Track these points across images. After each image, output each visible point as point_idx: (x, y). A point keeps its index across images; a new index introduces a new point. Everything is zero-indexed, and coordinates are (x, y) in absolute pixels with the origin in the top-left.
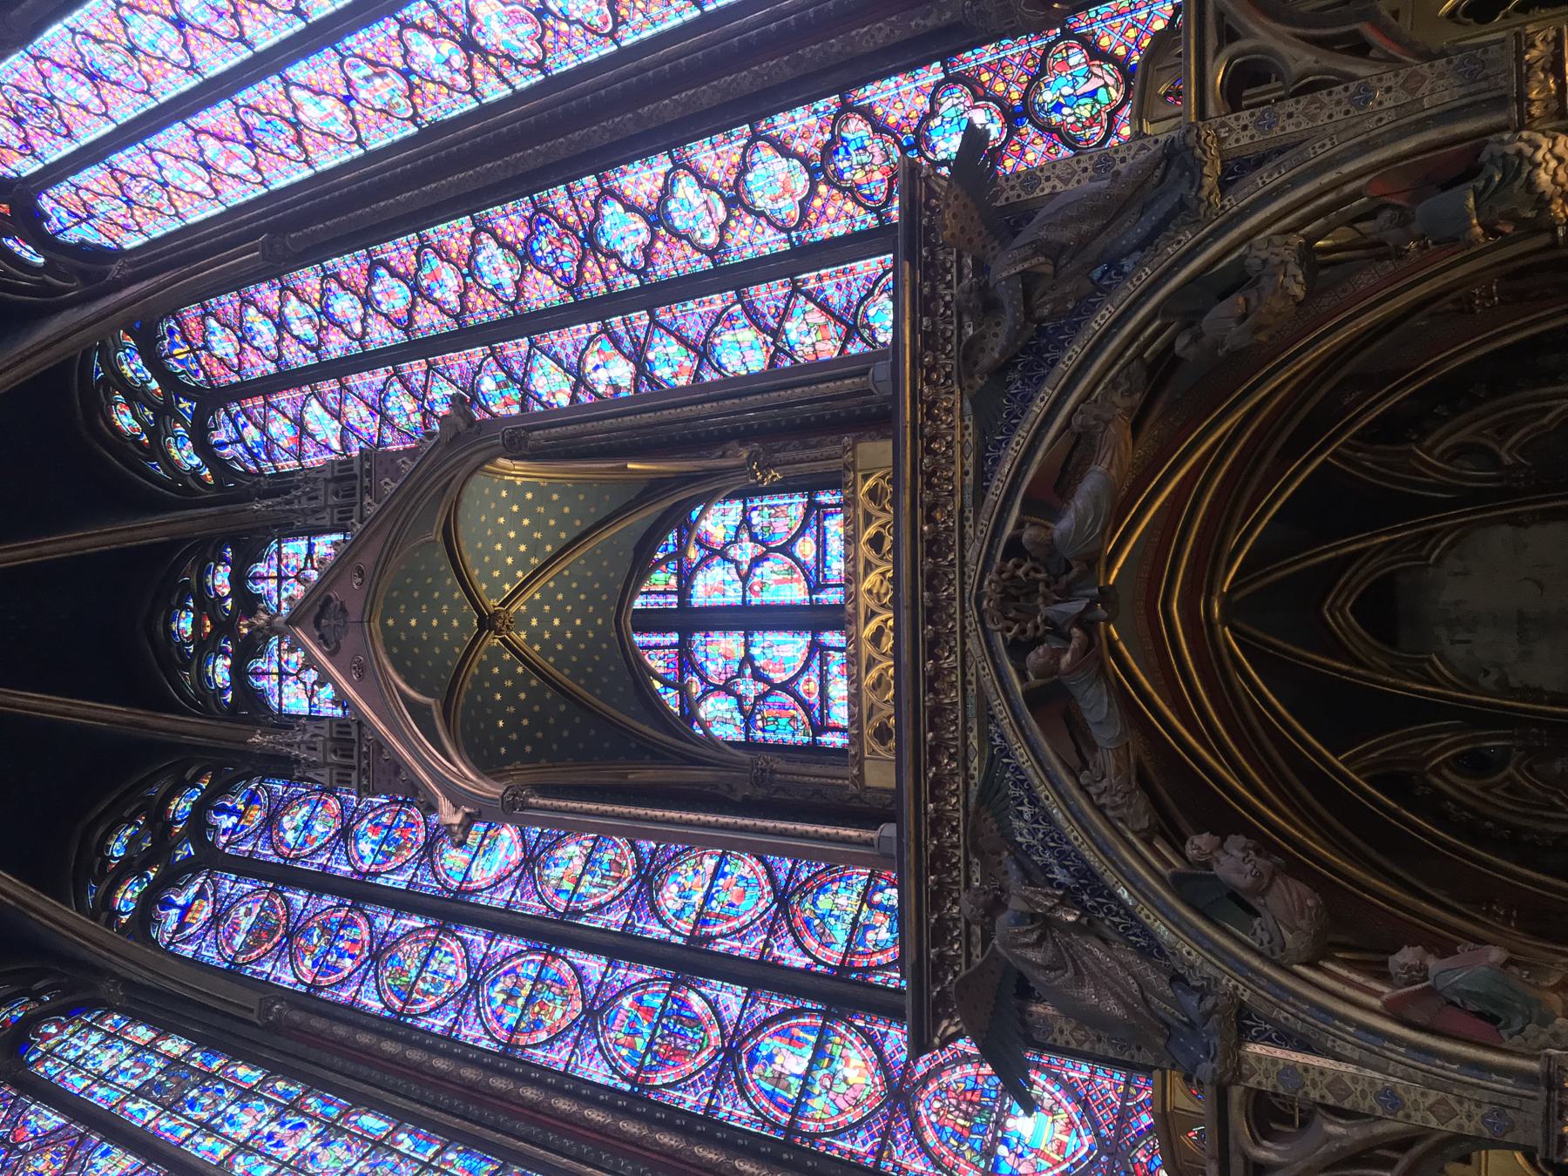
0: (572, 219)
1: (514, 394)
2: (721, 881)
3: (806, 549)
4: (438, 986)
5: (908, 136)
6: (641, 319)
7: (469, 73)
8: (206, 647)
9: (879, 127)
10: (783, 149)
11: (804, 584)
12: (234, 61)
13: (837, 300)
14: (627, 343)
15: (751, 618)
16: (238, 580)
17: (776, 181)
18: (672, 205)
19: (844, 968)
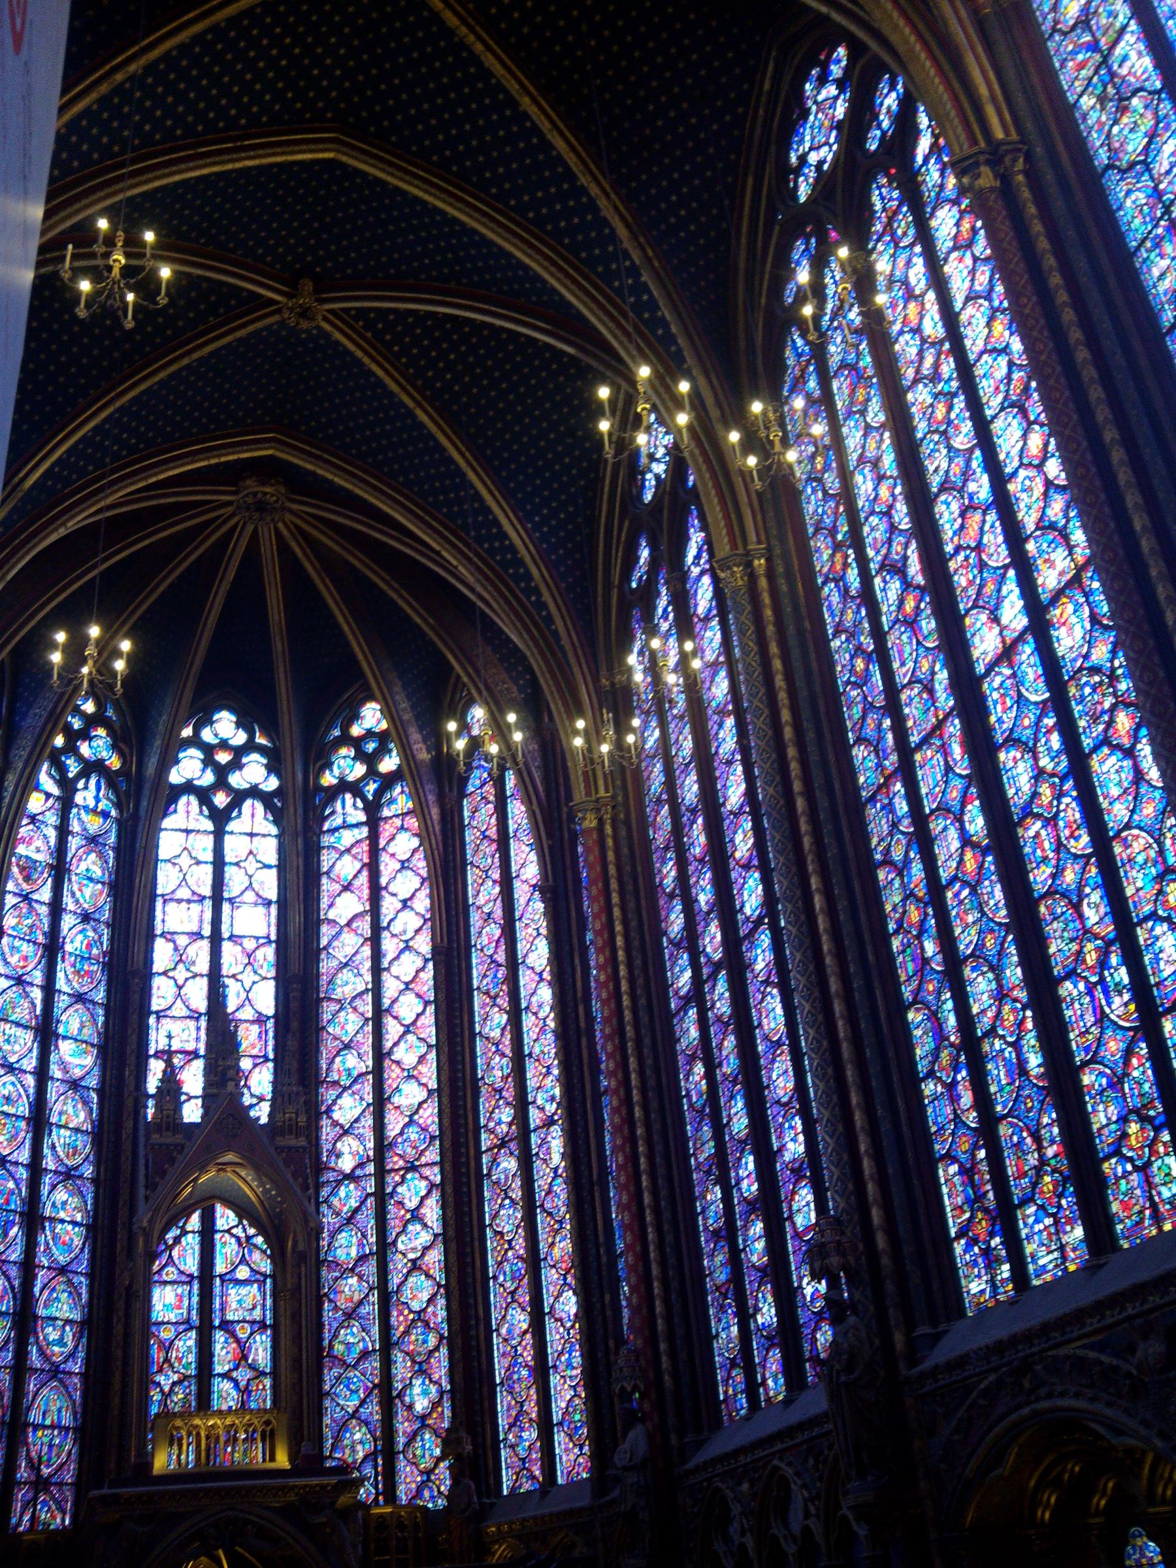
0: (423, 1160)
1: (345, 1082)
2: (70, 1227)
3: (243, 1273)
4: (8, 1041)
5: (425, 1366)
6: (370, 1186)
7: (492, 1131)
8: (209, 751)
9: (431, 1353)
10: (431, 1301)
11: (224, 1271)
12: (523, 993)
13: (364, 1310)
14: (358, 1172)
15: (208, 1233)
16: (254, 792)
17: (419, 1292)
18: (418, 1227)
19: (36, 1317)
